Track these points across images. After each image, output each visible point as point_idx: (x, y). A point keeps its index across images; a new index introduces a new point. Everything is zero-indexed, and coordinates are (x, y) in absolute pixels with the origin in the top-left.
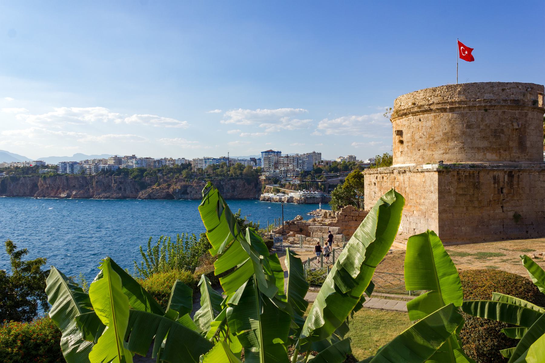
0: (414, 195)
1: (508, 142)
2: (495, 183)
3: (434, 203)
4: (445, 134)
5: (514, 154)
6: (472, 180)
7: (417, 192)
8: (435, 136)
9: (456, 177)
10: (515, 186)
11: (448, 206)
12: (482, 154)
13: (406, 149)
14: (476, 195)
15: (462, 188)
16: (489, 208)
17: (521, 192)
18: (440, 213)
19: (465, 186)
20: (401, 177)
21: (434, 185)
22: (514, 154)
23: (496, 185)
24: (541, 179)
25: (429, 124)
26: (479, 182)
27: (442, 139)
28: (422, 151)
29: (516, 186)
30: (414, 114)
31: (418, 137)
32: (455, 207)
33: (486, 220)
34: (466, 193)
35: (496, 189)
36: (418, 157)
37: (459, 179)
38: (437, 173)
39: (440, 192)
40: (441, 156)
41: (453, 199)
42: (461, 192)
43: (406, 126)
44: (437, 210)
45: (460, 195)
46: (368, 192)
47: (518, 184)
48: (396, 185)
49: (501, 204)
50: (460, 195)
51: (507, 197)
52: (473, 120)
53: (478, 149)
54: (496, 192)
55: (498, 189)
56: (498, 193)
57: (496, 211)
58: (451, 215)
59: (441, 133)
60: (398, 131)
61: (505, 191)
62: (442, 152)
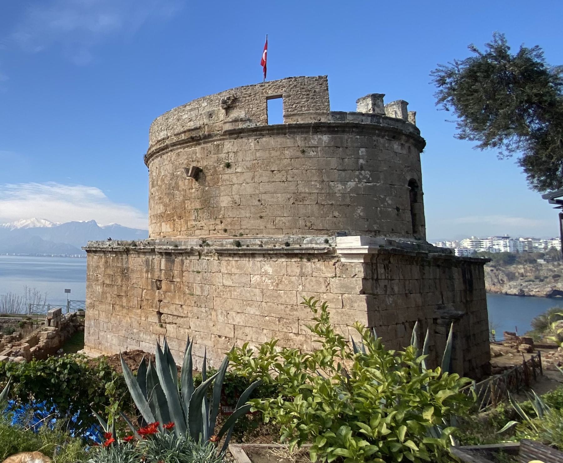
1: (184, 202)
2: (147, 272)
5: (194, 223)
6: (119, 265)
9: (103, 260)
14: (124, 288)
15: (109, 276)
16: (139, 311)
17: (187, 291)
19: (112, 273)
22: (194, 223)
23: (149, 276)
24: (224, 270)
26: (128, 269)
29: (178, 280)
32: (101, 302)
34: (113, 283)
35: (150, 281)
37: (106, 262)
41: (99, 289)
42: (108, 282)
45: (108, 285)
50: (108, 285)
51: (165, 298)
54: (149, 288)
56: (152, 289)
57: (149, 320)
58: (97, 312)
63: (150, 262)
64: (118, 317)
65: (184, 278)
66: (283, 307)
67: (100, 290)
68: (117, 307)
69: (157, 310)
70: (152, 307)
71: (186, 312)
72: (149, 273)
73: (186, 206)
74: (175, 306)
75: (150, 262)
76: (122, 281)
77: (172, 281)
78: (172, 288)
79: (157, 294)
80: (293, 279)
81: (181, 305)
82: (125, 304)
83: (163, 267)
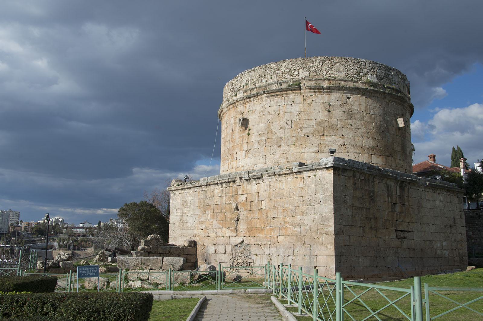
0: (280, 210)
2: (388, 196)
3: (325, 219)
4: (319, 124)
6: (367, 188)
7: (287, 206)
8: (305, 126)
9: (352, 181)
10: (406, 203)
11: (344, 223)
12: (367, 155)
13: (256, 146)
18: (338, 232)
19: (360, 195)
20: (252, 187)
21: (325, 190)
25: (297, 108)
26: (374, 192)
27: (315, 130)
28: (284, 147)
30: (271, 93)
31: (278, 127)
33: (382, 249)
35: (390, 204)
36: (277, 156)
37: (355, 184)
38: (332, 171)
39: (336, 202)
40: (314, 155)
42: (357, 204)
43: (257, 112)
44: (332, 229)
46: (178, 218)
47: (409, 201)
48: (240, 201)
49: (395, 226)
52: (356, 108)
53: (363, 147)
54: (390, 210)
55: (392, 205)
57: (391, 237)
59: (313, 123)
60: (244, 119)
61: (398, 208)
62: (316, 149)
63: (390, 188)
64: (368, 239)
65: (410, 202)
66: (446, 219)
67: (350, 213)
68: (367, 229)
69: (395, 229)
70: (392, 226)
71: (411, 228)
72: (390, 198)
73: (395, 147)
74: (406, 223)
75: (390, 188)
76: (370, 204)
77: (404, 205)
78: (404, 210)
79: (395, 214)
80: (448, 203)
81: (409, 222)
82: (373, 226)
83: (398, 194)
